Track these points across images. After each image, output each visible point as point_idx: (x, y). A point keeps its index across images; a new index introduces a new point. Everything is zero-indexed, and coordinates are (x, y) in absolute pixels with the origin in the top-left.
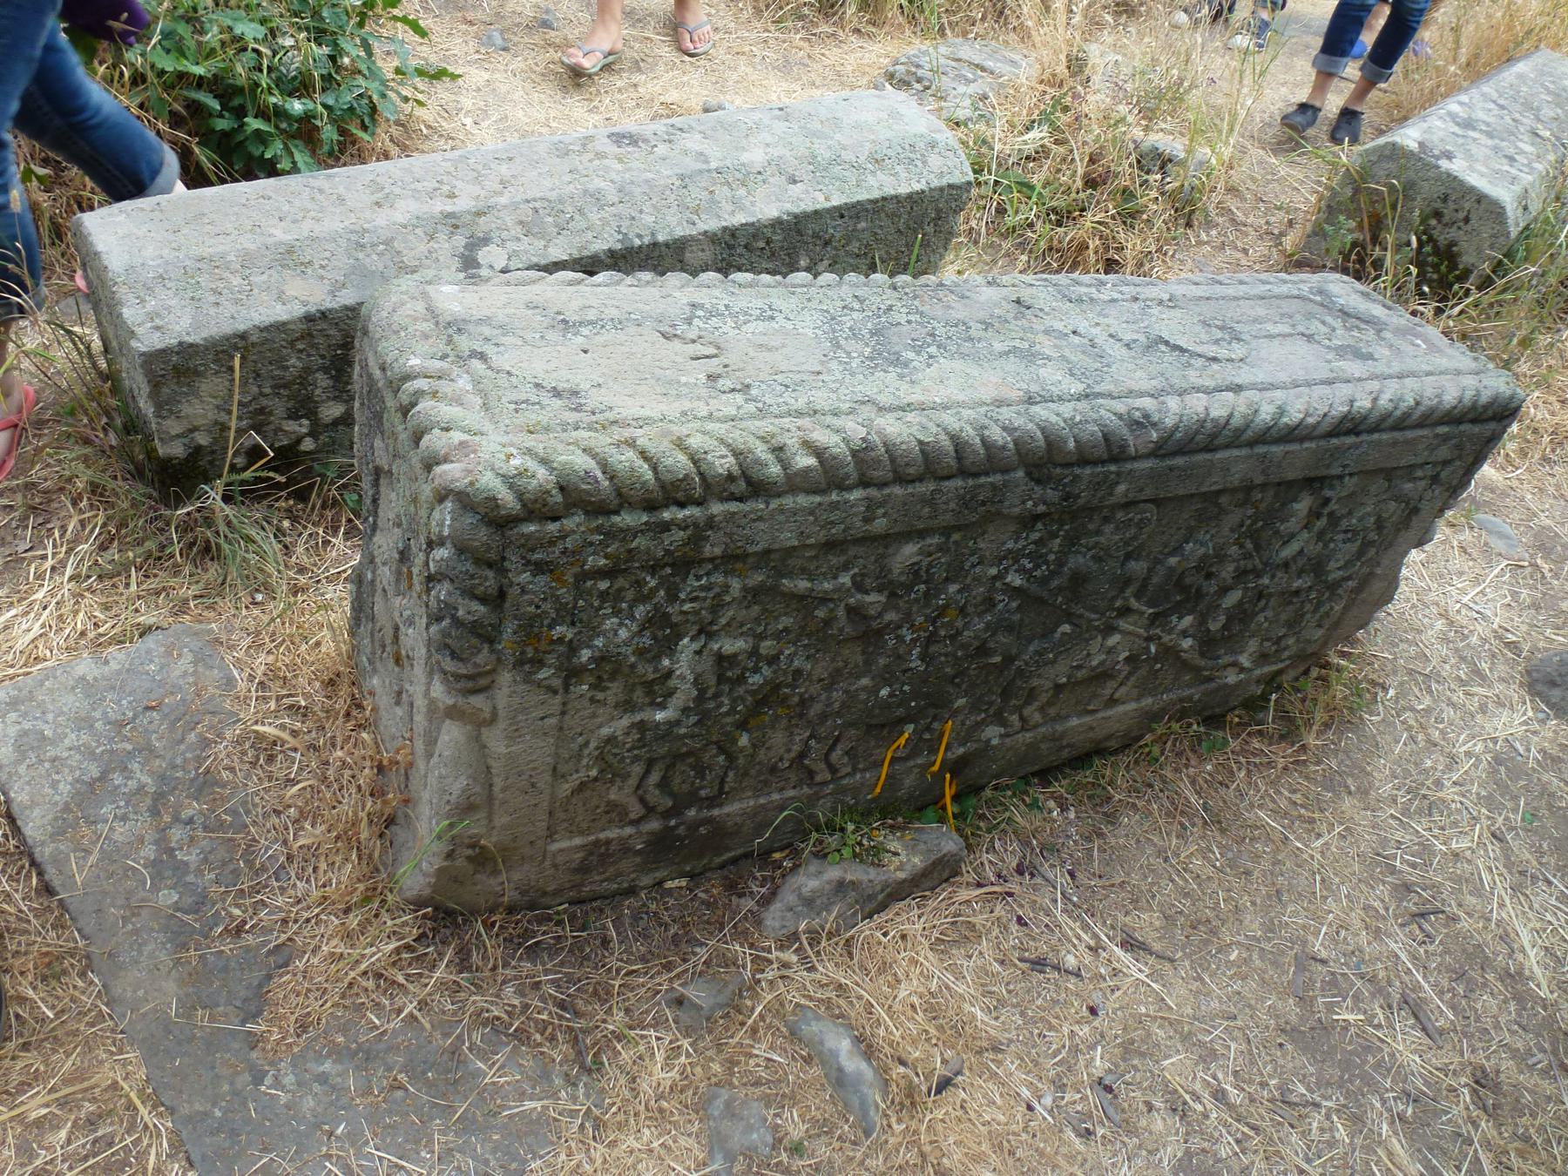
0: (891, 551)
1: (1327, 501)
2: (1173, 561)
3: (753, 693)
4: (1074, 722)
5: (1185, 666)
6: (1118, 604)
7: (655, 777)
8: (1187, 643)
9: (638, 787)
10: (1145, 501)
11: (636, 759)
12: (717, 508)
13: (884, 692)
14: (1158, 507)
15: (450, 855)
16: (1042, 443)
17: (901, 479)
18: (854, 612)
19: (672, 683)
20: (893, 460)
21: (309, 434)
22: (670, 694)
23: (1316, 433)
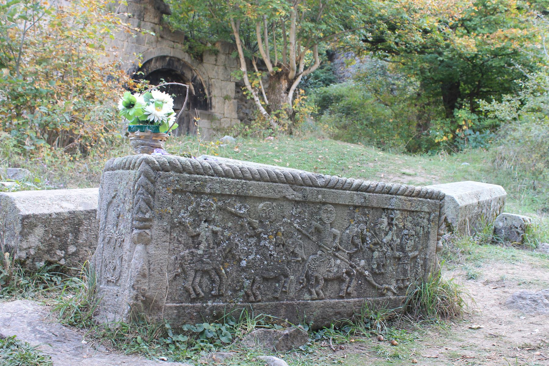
1: (392, 219)
2: (348, 231)
3: (225, 250)
6: (335, 245)
7: (198, 280)
8: (367, 273)
9: (192, 284)
15: (136, 298)
17: (254, 179)
19: (200, 239)
20: (251, 172)
21: (64, 257)
22: (199, 244)
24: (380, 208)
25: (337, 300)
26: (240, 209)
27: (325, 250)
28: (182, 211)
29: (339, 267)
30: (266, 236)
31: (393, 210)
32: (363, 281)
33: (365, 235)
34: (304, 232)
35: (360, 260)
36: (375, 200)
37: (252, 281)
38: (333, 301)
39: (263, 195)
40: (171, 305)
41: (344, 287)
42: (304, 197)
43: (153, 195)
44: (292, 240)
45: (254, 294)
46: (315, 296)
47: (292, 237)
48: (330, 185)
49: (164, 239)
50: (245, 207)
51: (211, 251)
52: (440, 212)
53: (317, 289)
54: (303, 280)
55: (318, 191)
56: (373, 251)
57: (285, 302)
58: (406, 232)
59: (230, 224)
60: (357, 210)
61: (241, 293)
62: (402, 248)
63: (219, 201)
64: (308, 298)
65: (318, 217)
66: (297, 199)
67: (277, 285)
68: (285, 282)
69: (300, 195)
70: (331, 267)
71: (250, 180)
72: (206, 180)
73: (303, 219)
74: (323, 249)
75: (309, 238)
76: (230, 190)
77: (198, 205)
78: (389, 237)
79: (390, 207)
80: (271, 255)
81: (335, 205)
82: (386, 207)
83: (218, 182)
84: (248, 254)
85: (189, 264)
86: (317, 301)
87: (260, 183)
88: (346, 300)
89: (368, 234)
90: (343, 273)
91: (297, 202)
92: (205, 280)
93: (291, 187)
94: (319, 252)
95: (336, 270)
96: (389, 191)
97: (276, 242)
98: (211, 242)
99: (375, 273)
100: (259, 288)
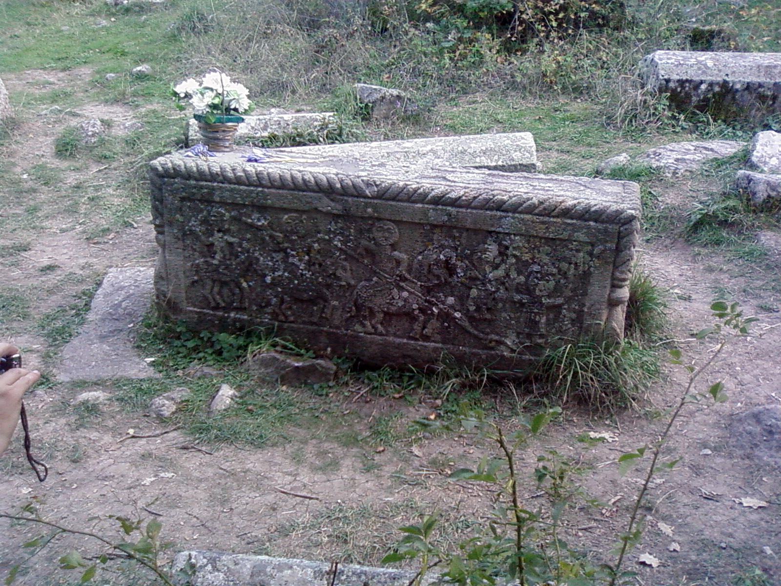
1: (507, 248)
2: (420, 257)
3: (243, 263)
7: (216, 289)
8: (457, 315)
9: (211, 292)
10: (388, 220)
11: (208, 277)
14: (398, 226)
17: (273, 186)
18: (271, 236)
20: (270, 179)
22: (215, 253)
24: (480, 230)
25: (405, 341)
26: (259, 220)
28: (193, 219)
29: (405, 300)
30: (294, 253)
31: (508, 234)
32: (451, 324)
33: (454, 264)
34: (349, 251)
35: (446, 297)
36: (468, 217)
38: (398, 340)
39: (285, 206)
40: (191, 309)
41: (417, 327)
42: (346, 210)
43: (161, 202)
44: (332, 260)
45: (284, 314)
46: (370, 329)
47: (331, 257)
48: (387, 195)
49: (176, 246)
50: (265, 219)
51: (228, 262)
52: (618, 244)
53: (373, 322)
54: (351, 308)
55: (366, 204)
56: (471, 288)
57: (325, 329)
58: (536, 268)
59: (249, 236)
60: (437, 231)
61: (269, 310)
62: (527, 289)
63: (233, 210)
64: (360, 330)
65: (371, 236)
66: (335, 212)
67: (315, 308)
68: (325, 306)
69: (340, 207)
70: (394, 299)
71: (269, 188)
72: (213, 189)
73: (348, 236)
74: (380, 276)
75: (358, 261)
76: (243, 199)
77: (209, 212)
78: (500, 272)
79: (500, 230)
80: (302, 275)
81: (398, 223)
82: (493, 229)
83: (228, 191)
84: (274, 270)
85: (205, 272)
86: (373, 336)
87: (281, 191)
88: (420, 343)
89: (459, 263)
91: (338, 216)
92: (225, 291)
93: (328, 197)
94: (375, 279)
95: (401, 304)
96: (501, 206)
97: (309, 261)
98: (228, 253)
99: (474, 317)
100: (290, 308)
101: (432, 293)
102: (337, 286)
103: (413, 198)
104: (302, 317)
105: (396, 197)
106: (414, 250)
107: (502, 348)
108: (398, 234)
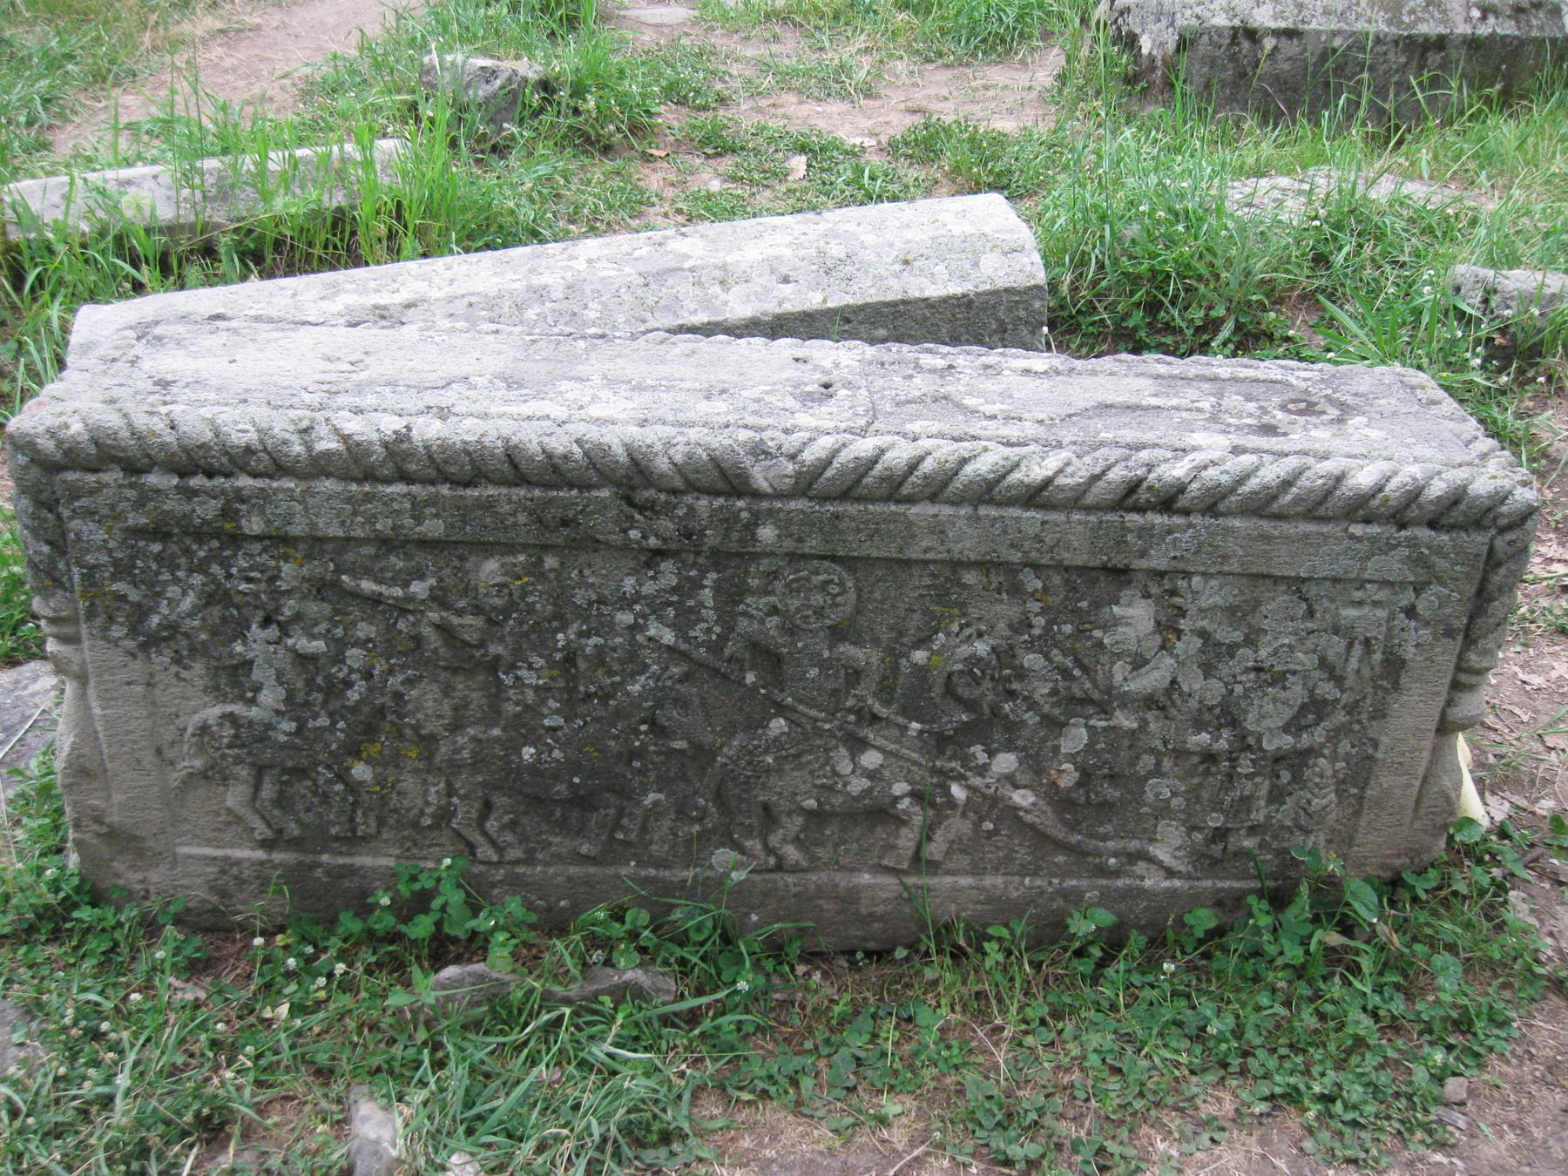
0: (468, 565)
2: (919, 656)
4: (866, 878)
5: (1040, 837)
7: (268, 790)
8: (1022, 798)
11: (238, 761)
12: (244, 482)
13: (528, 752)
14: (852, 570)
16: (623, 458)
22: (257, 689)
23: (1090, 499)
27: (804, 720)
29: (872, 775)
35: (991, 754)
37: (477, 805)
41: (906, 840)
53: (774, 840)
62: (1228, 716)
68: (621, 813)
72: (240, 497)
90: (896, 799)
95: (858, 785)
101: (948, 753)
102: (659, 753)
103: (905, 491)
104: (550, 844)
105: (850, 488)
106: (901, 634)
107: (1140, 868)
108: (852, 596)
